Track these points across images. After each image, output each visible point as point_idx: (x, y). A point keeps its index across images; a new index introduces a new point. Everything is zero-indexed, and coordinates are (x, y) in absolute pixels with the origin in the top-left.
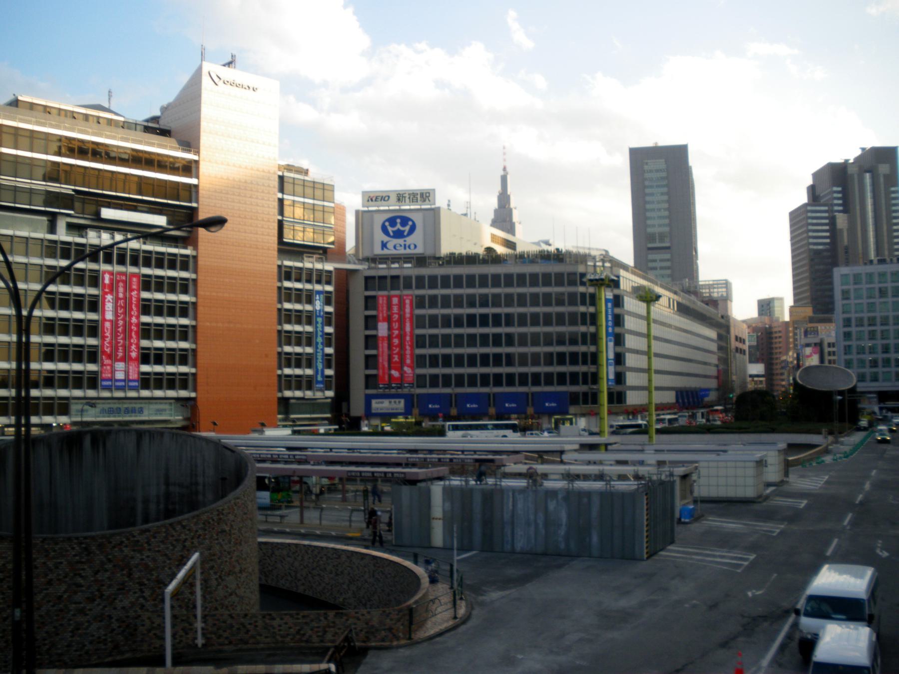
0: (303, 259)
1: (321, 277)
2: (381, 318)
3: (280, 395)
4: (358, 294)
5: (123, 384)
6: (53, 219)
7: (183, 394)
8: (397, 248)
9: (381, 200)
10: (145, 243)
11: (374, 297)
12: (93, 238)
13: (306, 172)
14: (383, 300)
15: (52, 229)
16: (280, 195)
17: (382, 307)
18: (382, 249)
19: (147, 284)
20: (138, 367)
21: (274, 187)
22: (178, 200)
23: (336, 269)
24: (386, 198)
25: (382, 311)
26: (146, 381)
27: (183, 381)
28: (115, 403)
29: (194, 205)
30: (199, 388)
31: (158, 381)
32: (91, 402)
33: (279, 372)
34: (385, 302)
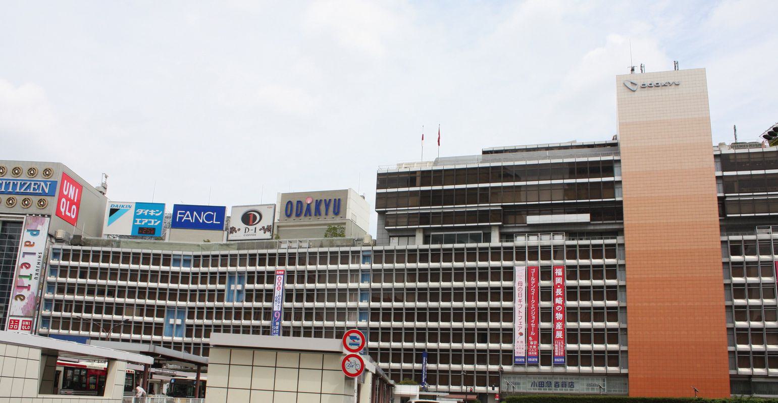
3: (733, 372)
12: (520, 241)
15: (488, 239)
16: (719, 174)
19: (572, 272)
20: (564, 346)
26: (572, 358)
27: (614, 358)
28: (546, 378)
29: (618, 199)
30: (629, 365)
31: (586, 358)
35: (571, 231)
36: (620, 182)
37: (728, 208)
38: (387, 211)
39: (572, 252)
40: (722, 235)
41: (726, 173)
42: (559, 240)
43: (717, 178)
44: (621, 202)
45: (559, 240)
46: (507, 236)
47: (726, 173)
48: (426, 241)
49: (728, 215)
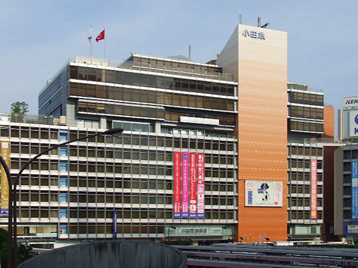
0: (304, 141)
1: (315, 151)
2: (354, 176)
3: (289, 222)
4: (338, 161)
5: (195, 215)
6: (153, 123)
7: (230, 221)
9: (355, 103)
10: (207, 136)
11: (350, 163)
12: (176, 133)
13: (306, 88)
14: (355, 165)
16: (289, 104)
17: (355, 169)
18: (355, 133)
19: (208, 158)
22: (226, 110)
23: (324, 147)
25: (355, 171)
27: (230, 214)
29: (236, 112)
31: (216, 214)
32: (173, 226)
33: (289, 209)
34: (356, 166)
35: (208, 129)
36: (237, 101)
37: (292, 126)
38: (78, 99)
39: (208, 145)
40: (288, 142)
41: (293, 104)
42: (200, 135)
43: (288, 106)
44: (236, 115)
45: (200, 135)
47: (293, 104)
49: (292, 130)
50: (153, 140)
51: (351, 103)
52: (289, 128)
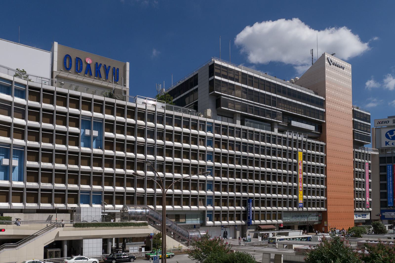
8: (394, 144)
9: (384, 123)
15: (272, 130)
21: (351, 115)
24: (387, 122)
34: (390, 168)
41: (355, 120)
46: (279, 131)
48: (242, 124)
50: (274, 139)
51: (382, 123)
52: (354, 138)
